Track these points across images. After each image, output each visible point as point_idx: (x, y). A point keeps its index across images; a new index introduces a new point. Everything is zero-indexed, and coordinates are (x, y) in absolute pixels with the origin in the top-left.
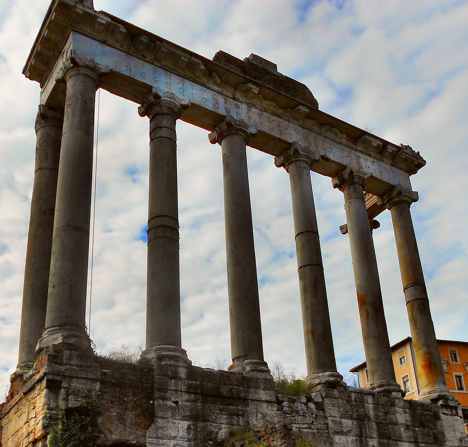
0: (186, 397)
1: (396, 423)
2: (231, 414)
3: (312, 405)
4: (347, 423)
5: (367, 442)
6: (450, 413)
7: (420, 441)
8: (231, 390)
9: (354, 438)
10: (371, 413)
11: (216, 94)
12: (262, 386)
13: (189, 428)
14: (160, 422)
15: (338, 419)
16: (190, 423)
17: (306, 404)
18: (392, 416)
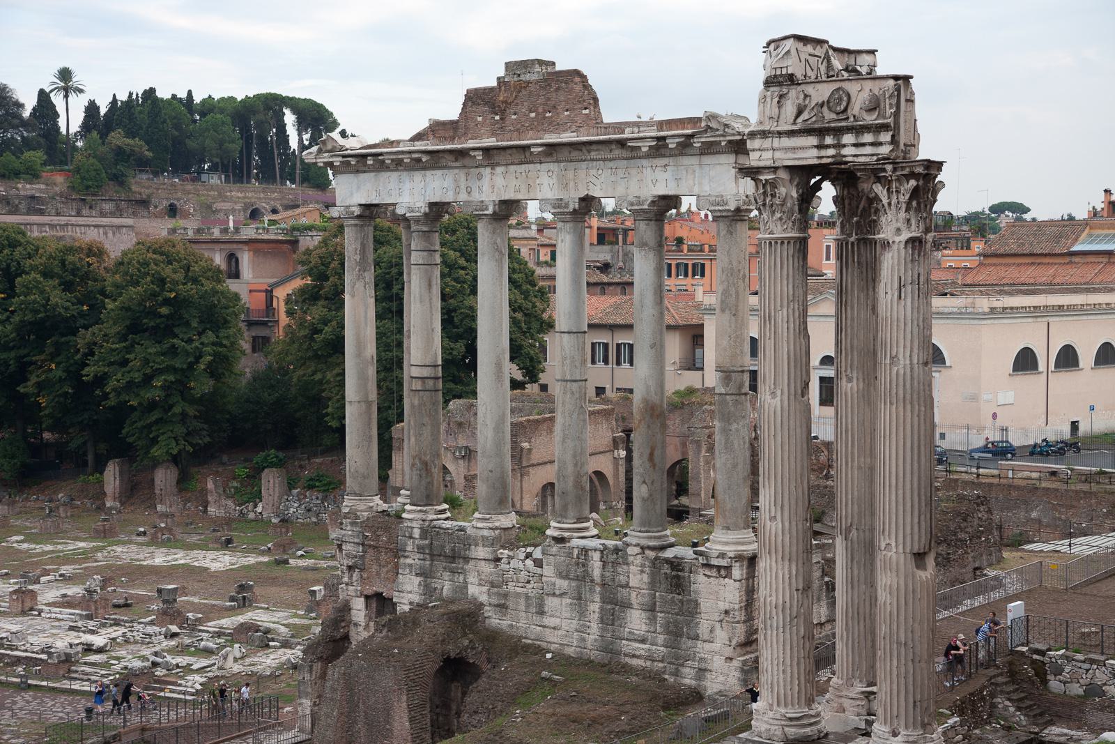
1: (627, 586)
3: (529, 562)
4: (562, 584)
5: (586, 605)
6: (714, 574)
7: (658, 609)
8: (453, 550)
9: (569, 601)
10: (597, 573)
11: (456, 171)
12: (481, 544)
13: (420, 584)
15: (553, 580)
16: (422, 579)
17: (523, 561)
18: (621, 577)
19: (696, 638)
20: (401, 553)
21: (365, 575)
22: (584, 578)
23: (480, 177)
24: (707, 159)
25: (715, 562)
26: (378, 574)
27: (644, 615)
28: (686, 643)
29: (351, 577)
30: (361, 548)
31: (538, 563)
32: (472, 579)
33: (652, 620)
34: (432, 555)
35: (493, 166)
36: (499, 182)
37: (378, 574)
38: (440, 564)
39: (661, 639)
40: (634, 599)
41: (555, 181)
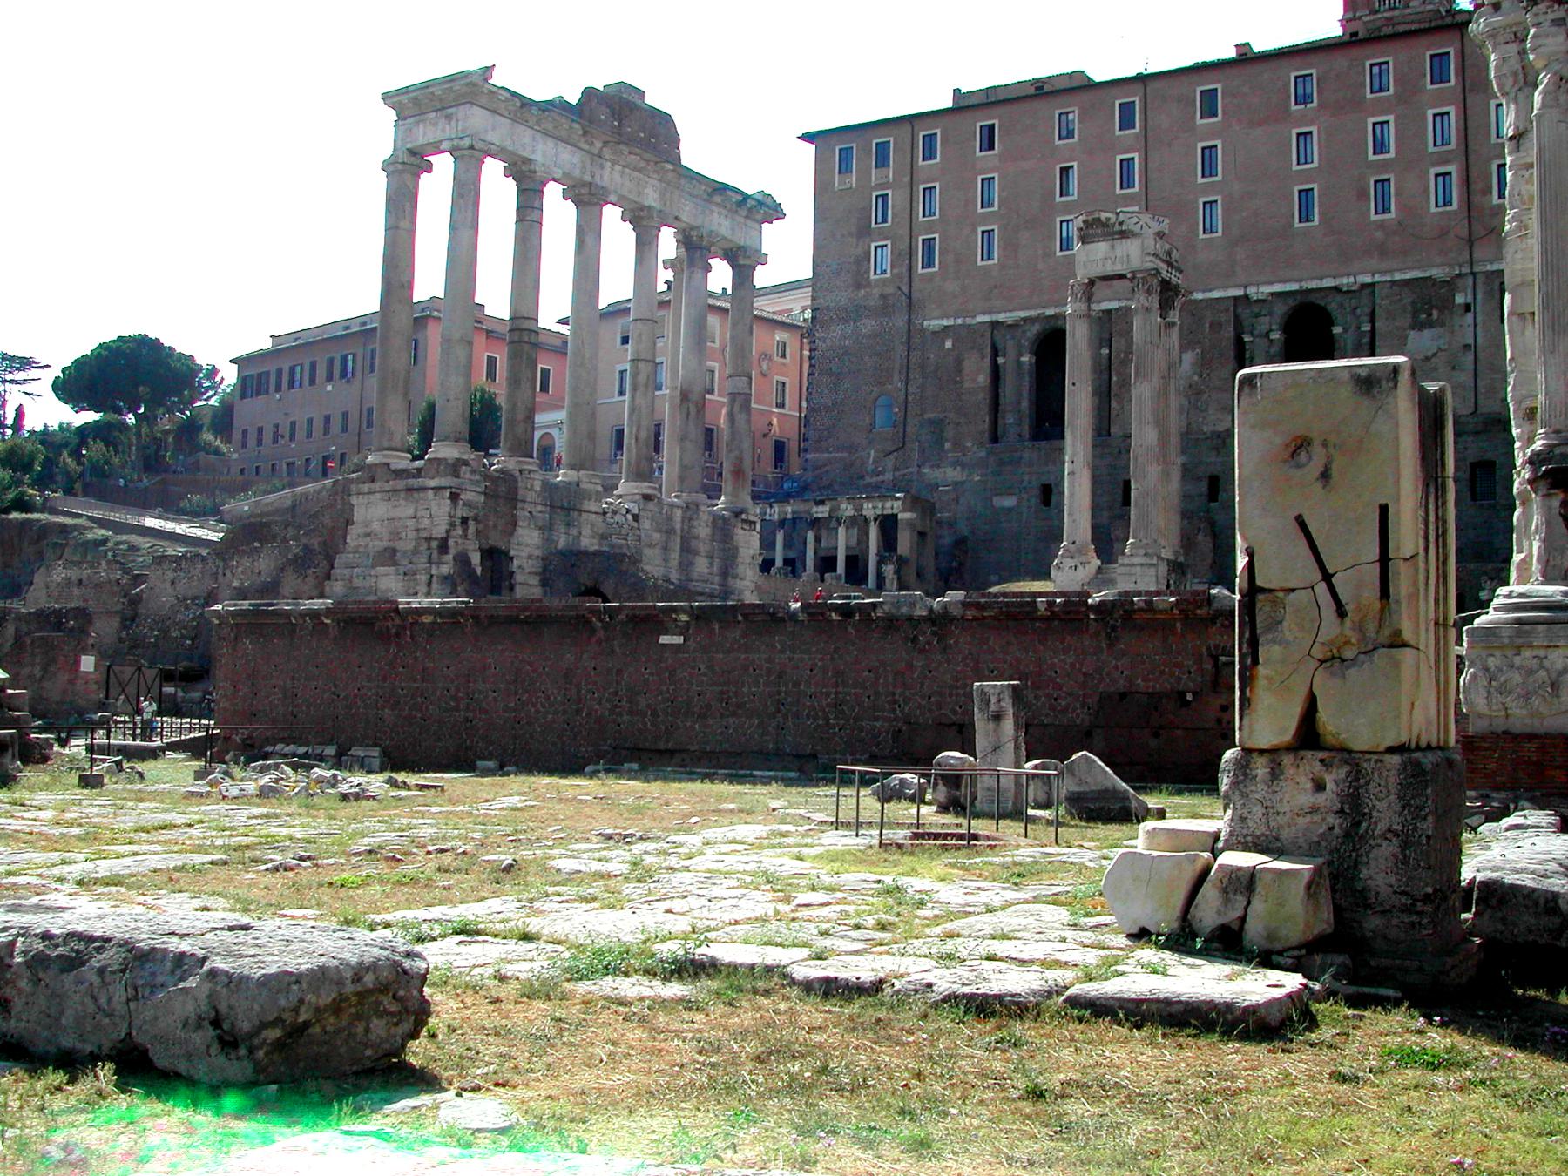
0: (540, 508)
1: (696, 538)
2: (568, 525)
3: (629, 517)
4: (657, 536)
10: (678, 526)
14: (520, 531)
19: (735, 577)
20: (520, 505)
21: (481, 527)
22: (670, 532)
23: (602, 167)
24: (749, 223)
25: (752, 518)
26: (495, 526)
27: (706, 561)
28: (731, 581)
29: (465, 531)
30: (482, 498)
31: (636, 518)
32: (586, 531)
33: (711, 564)
34: (552, 506)
35: (614, 163)
36: (617, 176)
37: (495, 526)
38: (559, 518)
39: (717, 579)
40: (703, 548)
41: (656, 196)
